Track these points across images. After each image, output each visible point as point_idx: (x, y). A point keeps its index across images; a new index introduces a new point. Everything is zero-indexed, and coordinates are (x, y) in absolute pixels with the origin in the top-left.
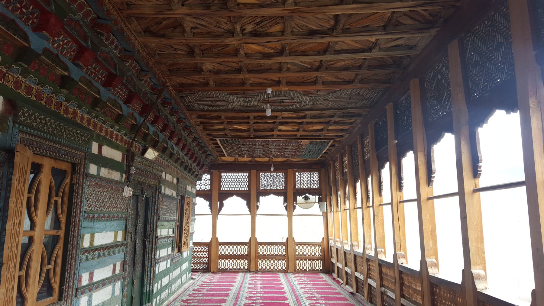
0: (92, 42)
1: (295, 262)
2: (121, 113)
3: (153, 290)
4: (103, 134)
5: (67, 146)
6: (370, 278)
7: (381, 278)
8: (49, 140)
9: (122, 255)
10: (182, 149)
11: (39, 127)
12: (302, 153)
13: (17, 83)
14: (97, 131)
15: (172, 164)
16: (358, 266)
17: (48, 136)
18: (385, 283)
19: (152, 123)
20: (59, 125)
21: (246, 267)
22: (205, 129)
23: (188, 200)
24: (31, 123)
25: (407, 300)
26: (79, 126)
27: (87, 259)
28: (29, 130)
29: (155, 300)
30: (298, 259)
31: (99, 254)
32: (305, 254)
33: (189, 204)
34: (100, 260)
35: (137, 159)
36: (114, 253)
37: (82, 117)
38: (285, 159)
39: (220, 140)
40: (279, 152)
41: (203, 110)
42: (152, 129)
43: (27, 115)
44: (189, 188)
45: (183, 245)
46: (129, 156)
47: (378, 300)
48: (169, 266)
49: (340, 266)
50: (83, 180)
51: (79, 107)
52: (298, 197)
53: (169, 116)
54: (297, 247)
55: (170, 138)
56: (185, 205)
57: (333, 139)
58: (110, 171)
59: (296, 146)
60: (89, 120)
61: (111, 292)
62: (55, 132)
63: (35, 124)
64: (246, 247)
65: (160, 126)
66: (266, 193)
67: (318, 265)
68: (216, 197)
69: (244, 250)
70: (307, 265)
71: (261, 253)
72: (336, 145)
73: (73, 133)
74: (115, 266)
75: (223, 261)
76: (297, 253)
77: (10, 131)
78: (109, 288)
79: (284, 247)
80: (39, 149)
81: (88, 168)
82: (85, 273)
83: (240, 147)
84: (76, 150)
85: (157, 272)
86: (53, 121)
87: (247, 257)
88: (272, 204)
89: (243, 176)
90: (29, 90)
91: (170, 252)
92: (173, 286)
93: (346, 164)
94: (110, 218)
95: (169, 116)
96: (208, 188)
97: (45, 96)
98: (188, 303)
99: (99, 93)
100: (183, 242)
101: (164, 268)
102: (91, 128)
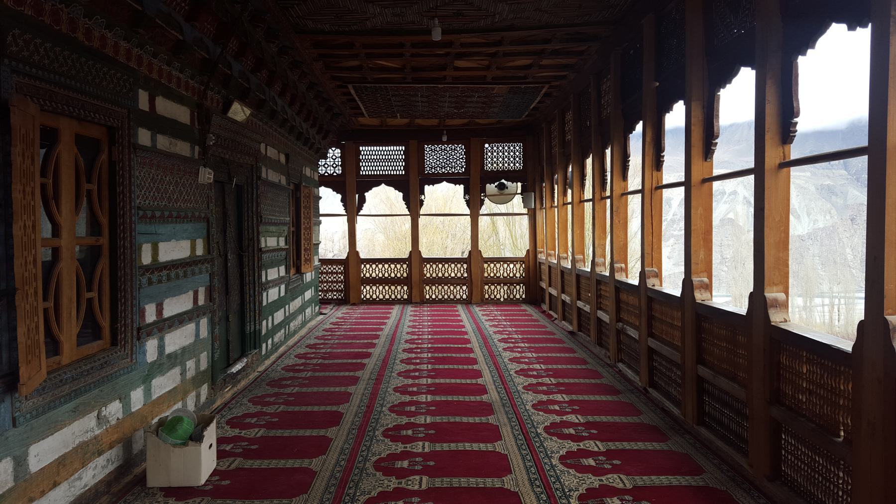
1: (483, 288)
2: (181, 38)
3: (260, 331)
4: (155, 76)
6: (601, 309)
7: (618, 309)
9: (205, 277)
12: (496, 110)
15: (276, 130)
16: (583, 292)
18: (624, 316)
21: (406, 297)
23: (307, 191)
25: (657, 340)
27: (150, 283)
29: (264, 345)
30: (487, 284)
31: (168, 275)
32: (498, 275)
33: (309, 197)
35: (216, 119)
36: (193, 274)
38: (466, 121)
39: (354, 88)
40: (456, 108)
44: (308, 172)
45: (303, 262)
46: (202, 115)
47: (612, 341)
48: (282, 294)
49: (554, 292)
50: (129, 155)
52: (488, 185)
54: (486, 266)
56: (302, 199)
57: (549, 83)
58: (173, 141)
59: (485, 97)
61: (194, 332)
64: (405, 266)
66: (435, 179)
67: (519, 292)
68: (353, 189)
69: (401, 271)
70: (501, 292)
71: (428, 275)
72: (555, 94)
75: (368, 288)
76: (486, 275)
78: (191, 327)
79: (465, 266)
81: (136, 135)
82: (150, 305)
83: (390, 100)
85: (265, 303)
87: (405, 281)
88: (445, 197)
89: (397, 151)
91: (283, 272)
92: (292, 324)
93: (569, 126)
94: (180, 217)
96: (339, 171)
98: (316, 348)
100: (303, 259)
101: (276, 297)
102: (133, 65)
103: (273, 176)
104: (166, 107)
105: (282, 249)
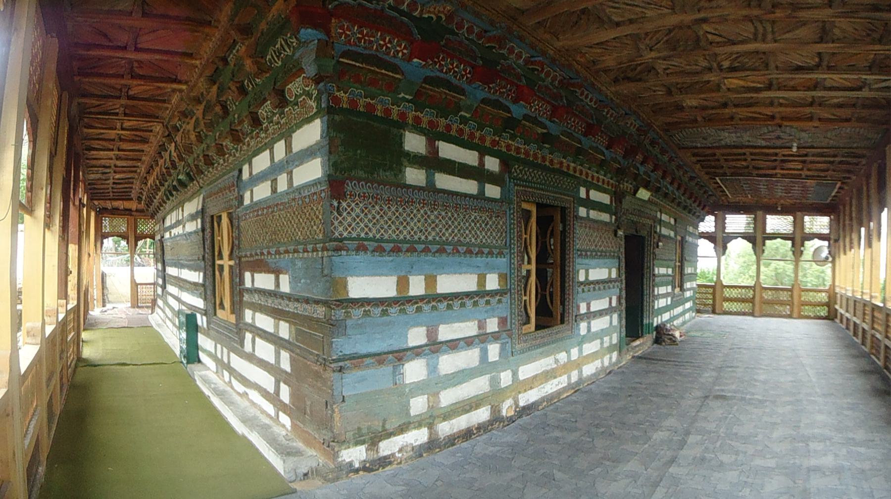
0: (567, 100)
4: (590, 179)
10: (678, 189)
13: (508, 147)
14: (584, 177)
19: (642, 164)
22: (703, 167)
26: (567, 175)
34: (596, 292)
36: (609, 288)
37: (568, 166)
41: (696, 148)
42: (642, 169)
53: (659, 156)
55: (663, 177)
60: (575, 169)
65: (650, 166)
74: (611, 299)
81: (578, 211)
84: (565, 195)
90: (518, 150)
95: (659, 156)
97: (532, 153)
99: (580, 142)
101: (664, 305)
102: (577, 175)
103: (665, 231)
104: (595, 195)
105: (669, 276)
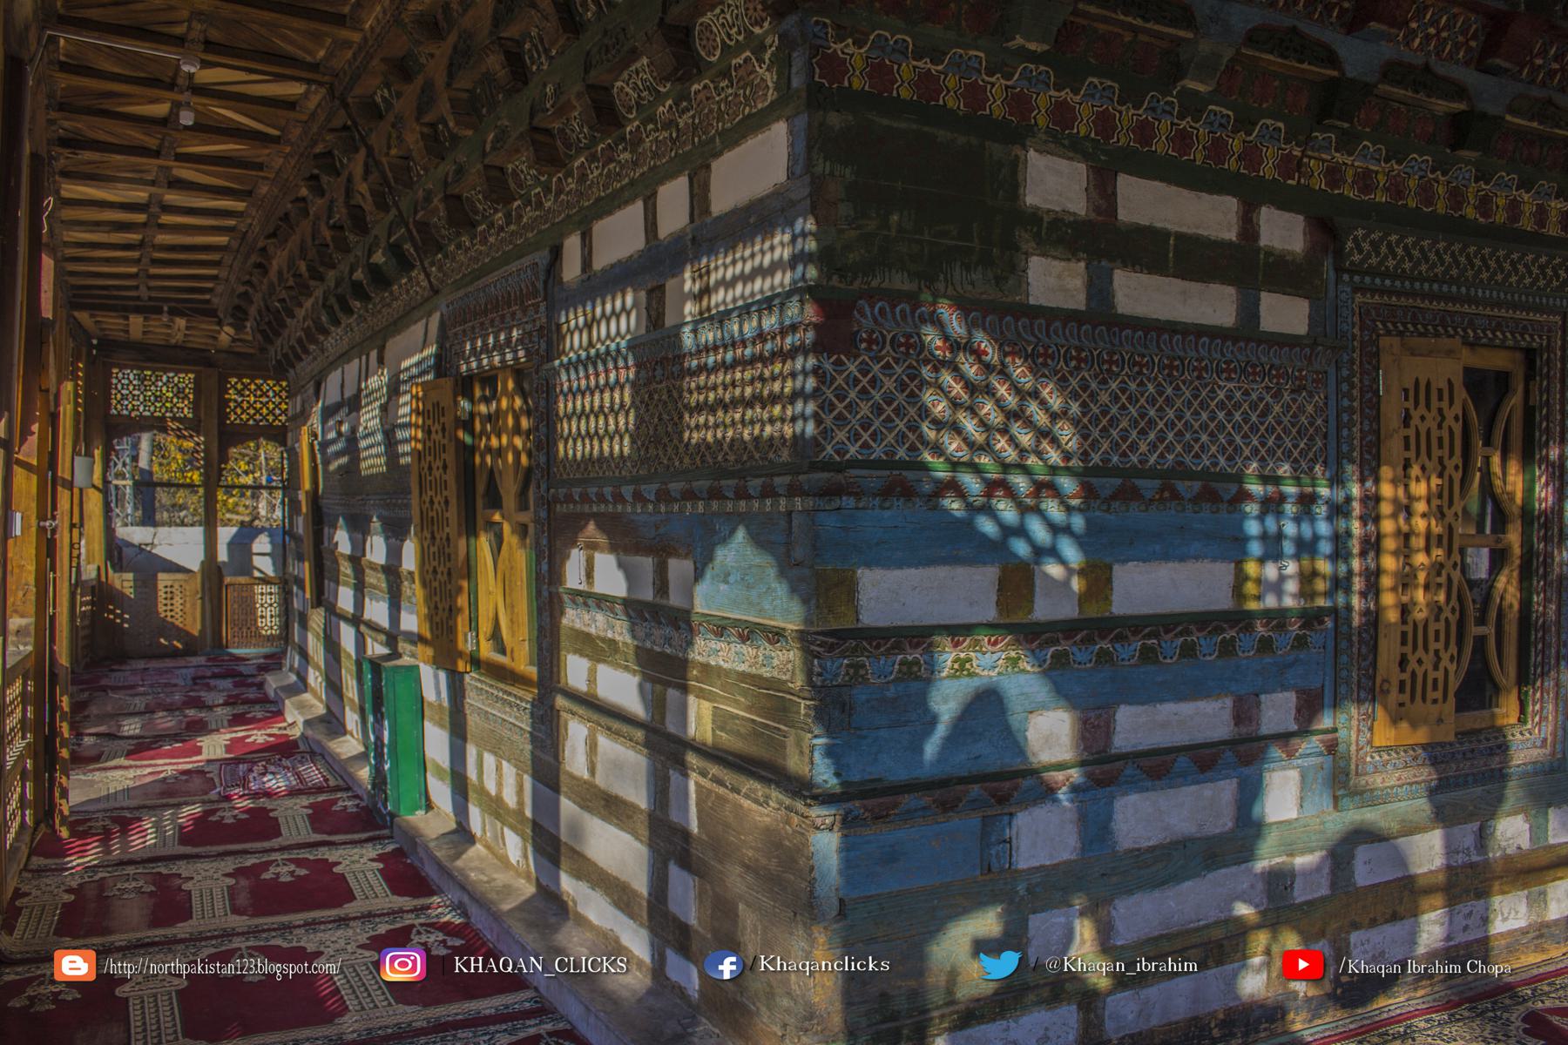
5: (1498, 304)
8: (1432, 297)
11: (1404, 271)
13: (1334, 174)
17: (1435, 286)
20: (1462, 251)
24: (1380, 263)
26: (1535, 240)
28: (1378, 281)
43: (1366, 246)
51: (1525, 185)
62: (1454, 272)
63: (1391, 263)
73: (1513, 263)
77: (1331, 294)
80: (1415, 325)
84: (1528, 308)
86: (1441, 245)
90: (1365, 181)
